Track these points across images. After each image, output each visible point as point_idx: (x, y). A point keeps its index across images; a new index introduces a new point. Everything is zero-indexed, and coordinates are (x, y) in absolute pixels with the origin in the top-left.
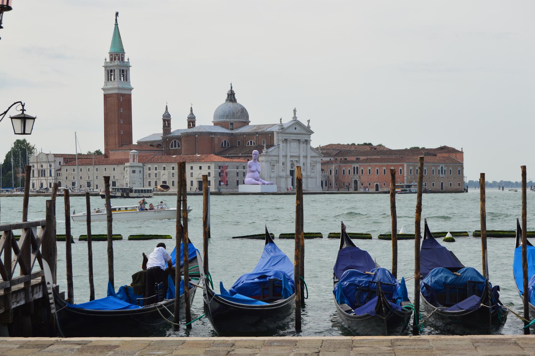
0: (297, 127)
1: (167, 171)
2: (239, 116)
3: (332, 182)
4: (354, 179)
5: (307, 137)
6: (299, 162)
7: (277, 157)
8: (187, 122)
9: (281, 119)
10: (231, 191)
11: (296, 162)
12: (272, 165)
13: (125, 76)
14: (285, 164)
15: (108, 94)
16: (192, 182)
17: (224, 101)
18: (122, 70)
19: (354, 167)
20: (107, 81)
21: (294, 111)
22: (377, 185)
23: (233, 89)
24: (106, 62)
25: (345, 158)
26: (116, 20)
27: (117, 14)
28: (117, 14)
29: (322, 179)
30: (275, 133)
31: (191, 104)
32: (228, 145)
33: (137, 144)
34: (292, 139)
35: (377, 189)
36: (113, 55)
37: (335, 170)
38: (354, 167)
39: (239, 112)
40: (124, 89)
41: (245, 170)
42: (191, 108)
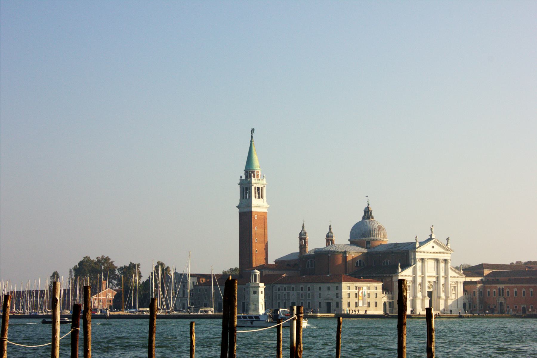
0: (435, 245)
1: (296, 291)
3: (476, 305)
4: (500, 301)
5: (446, 256)
6: (438, 282)
8: (326, 240)
9: (416, 237)
13: (261, 193)
15: (243, 212)
16: (320, 303)
17: (361, 219)
18: (258, 187)
19: (500, 288)
20: (242, 199)
21: (431, 229)
22: (524, 308)
23: (370, 206)
24: (240, 180)
25: (497, 278)
26: (252, 137)
27: (253, 130)
28: (253, 130)
29: (465, 301)
30: (410, 251)
32: (364, 265)
33: (274, 263)
35: (524, 312)
36: (249, 172)
37: (479, 292)
38: (500, 288)
39: (375, 230)
41: (376, 291)
42: (330, 226)
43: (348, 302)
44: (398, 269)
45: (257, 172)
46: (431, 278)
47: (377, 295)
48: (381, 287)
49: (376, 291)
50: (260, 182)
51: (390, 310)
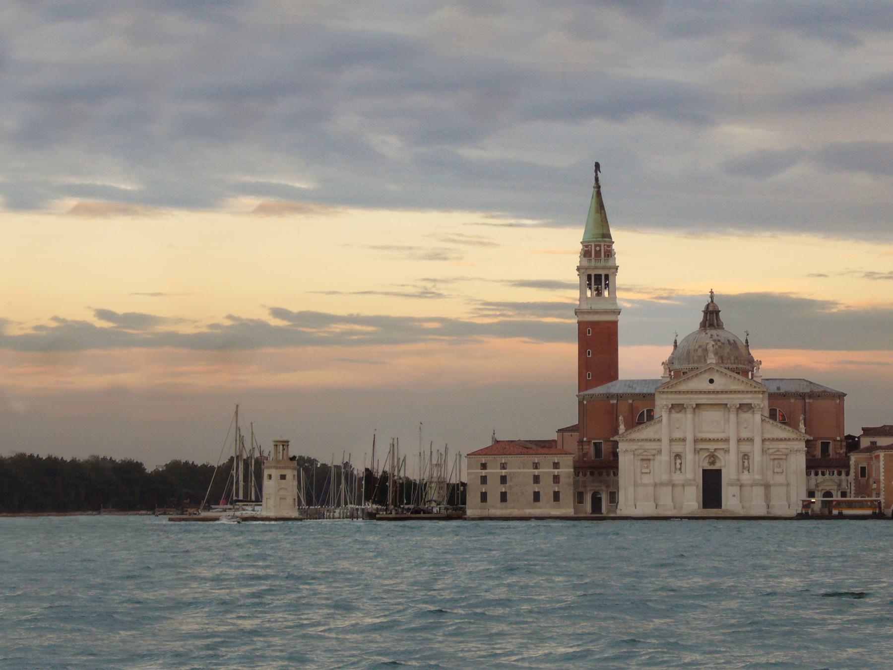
0: (716, 377)
2: (699, 357)
5: (749, 398)
7: (659, 443)
10: (516, 512)
11: (722, 452)
12: (642, 460)
14: (683, 455)
17: (697, 327)
23: (714, 302)
26: (597, 179)
27: (597, 166)
28: (597, 166)
29: (828, 488)
31: (745, 334)
34: (697, 405)
37: (856, 469)
40: (597, 312)
43: (482, 493)
44: (618, 426)
45: (596, 246)
46: (712, 443)
47: (562, 479)
48: (571, 463)
49: (556, 471)
50: (602, 264)
51: (611, 506)
